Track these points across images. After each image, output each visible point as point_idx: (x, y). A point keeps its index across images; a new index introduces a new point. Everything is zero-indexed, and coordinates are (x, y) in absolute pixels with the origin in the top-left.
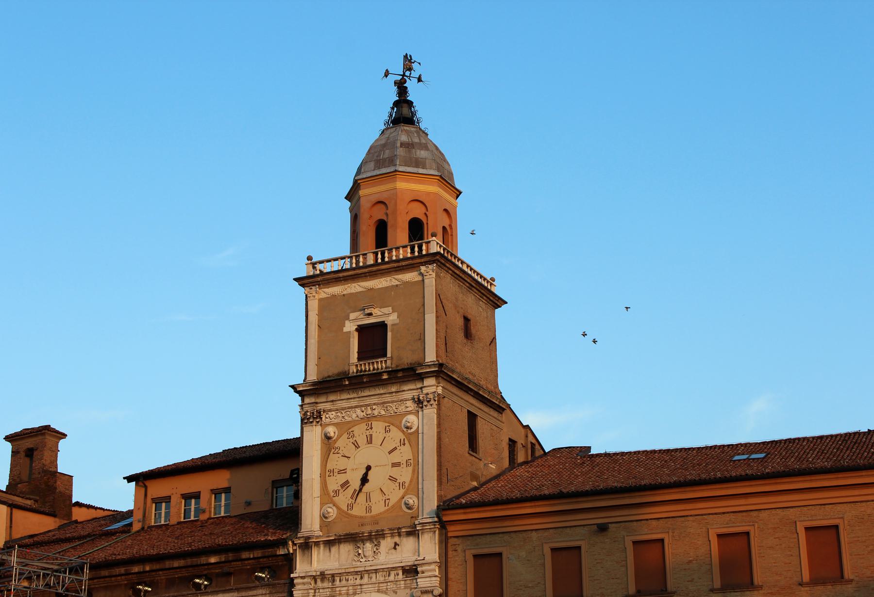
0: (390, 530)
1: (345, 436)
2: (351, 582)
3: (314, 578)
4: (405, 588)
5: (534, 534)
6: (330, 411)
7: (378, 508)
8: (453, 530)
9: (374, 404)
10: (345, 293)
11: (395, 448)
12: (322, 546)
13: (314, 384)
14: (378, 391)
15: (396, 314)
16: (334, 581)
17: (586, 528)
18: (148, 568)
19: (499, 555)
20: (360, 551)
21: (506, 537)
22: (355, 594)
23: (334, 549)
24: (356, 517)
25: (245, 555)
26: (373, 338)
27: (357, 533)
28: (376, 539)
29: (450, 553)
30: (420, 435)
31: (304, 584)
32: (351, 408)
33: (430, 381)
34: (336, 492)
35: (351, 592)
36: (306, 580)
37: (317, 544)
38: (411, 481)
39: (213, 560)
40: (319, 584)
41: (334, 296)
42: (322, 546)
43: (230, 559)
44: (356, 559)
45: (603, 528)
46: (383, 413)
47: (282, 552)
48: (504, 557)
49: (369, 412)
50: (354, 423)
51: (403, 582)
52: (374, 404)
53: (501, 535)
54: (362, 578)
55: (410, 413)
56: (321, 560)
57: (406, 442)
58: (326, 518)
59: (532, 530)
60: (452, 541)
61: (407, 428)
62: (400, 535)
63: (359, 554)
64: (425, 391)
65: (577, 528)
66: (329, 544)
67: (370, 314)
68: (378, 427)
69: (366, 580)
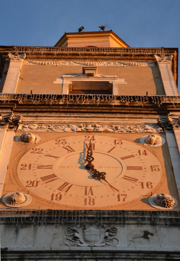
15: (122, 81)
20: (77, 235)
28: (109, 224)
44: (67, 242)
52: (98, 123)
57: (147, 152)
62: (153, 224)
63: (76, 238)
67: (91, 75)
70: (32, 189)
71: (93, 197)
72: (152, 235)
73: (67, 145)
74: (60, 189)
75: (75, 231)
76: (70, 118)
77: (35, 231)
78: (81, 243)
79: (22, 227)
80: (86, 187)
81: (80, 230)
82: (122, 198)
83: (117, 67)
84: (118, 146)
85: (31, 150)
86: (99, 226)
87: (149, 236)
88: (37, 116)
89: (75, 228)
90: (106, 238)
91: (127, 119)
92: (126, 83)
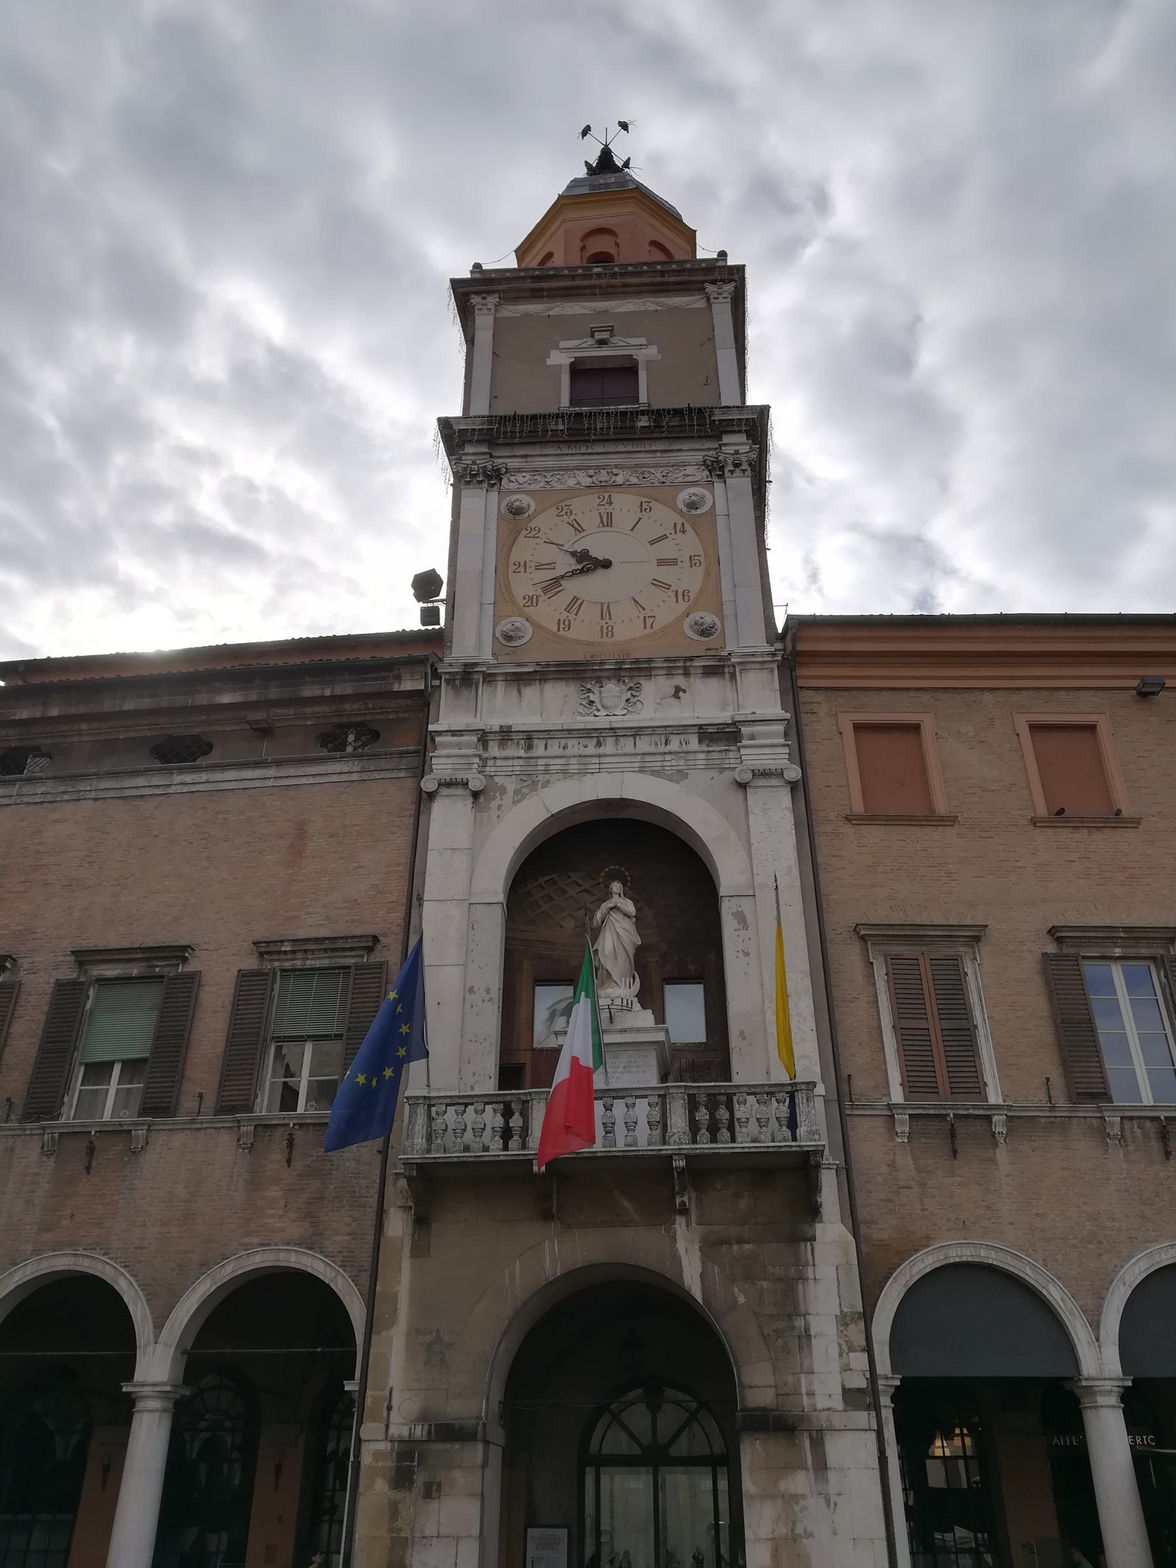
0: (668, 660)
1: (553, 511)
2: (576, 751)
3: (484, 737)
4: (708, 768)
5: (987, 697)
6: (519, 470)
7: (628, 631)
8: (808, 675)
9: (616, 466)
10: (551, 313)
11: (665, 537)
12: (500, 686)
13: (491, 419)
14: (621, 448)
15: (652, 351)
16: (530, 747)
17: (1101, 693)
18: (54, 712)
19: (915, 729)
20: (592, 698)
21: (925, 697)
22: (583, 773)
23: (530, 693)
24: (577, 642)
25: (310, 691)
26: (603, 377)
27: (587, 663)
28: (631, 677)
29: (805, 718)
30: (721, 521)
31: (459, 746)
32: (567, 469)
33: (742, 438)
34: (532, 600)
35: (574, 766)
36: (465, 738)
37: (489, 678)
38: (702, 590)
39: (226, 699)
40: (494, 750)
41: (527, 316)
42: (500, 686)
43: (272, 697)
45: (1145, 693)
46: (634, 480)
47: (407, 685)
48: (927, 730)
49: (604, 476)
50: (573, 493)
51: (702, 756)
52: (616, 466)
53: (912, 694)
54: (599, 744)
55: (694, 484)
56: (499, 708)
57: (687, 527)
58: (509, 638)
59: (983, 689)
60: (805, 696)
61: (692, 505)
62: (687, 673)
64: (725, 449)
65: (1084, 693)
66: (519, 680)
67: (602, 343)
68: (625, 505)
69: (609, 747)
70: (531, 611)
71: (611, 623)
72: (685, 691)
73: (573, 517)
74: (568, 610)
75: (589, 690)
76: (574, 458)
77: (542, 691)
78: (598, 710)
79: (526, 685)
80: (602, 604)
81: (596, 689)
82: (649, 621)
83: (646, 312)
84: (646, 515)
85: (524, 532)
86: (619, 679)
87: (681, 694)
88: (526, 456)
89: (589, 686)
90: (627, 700)
91: (658, 454)
92: (659, 357)
